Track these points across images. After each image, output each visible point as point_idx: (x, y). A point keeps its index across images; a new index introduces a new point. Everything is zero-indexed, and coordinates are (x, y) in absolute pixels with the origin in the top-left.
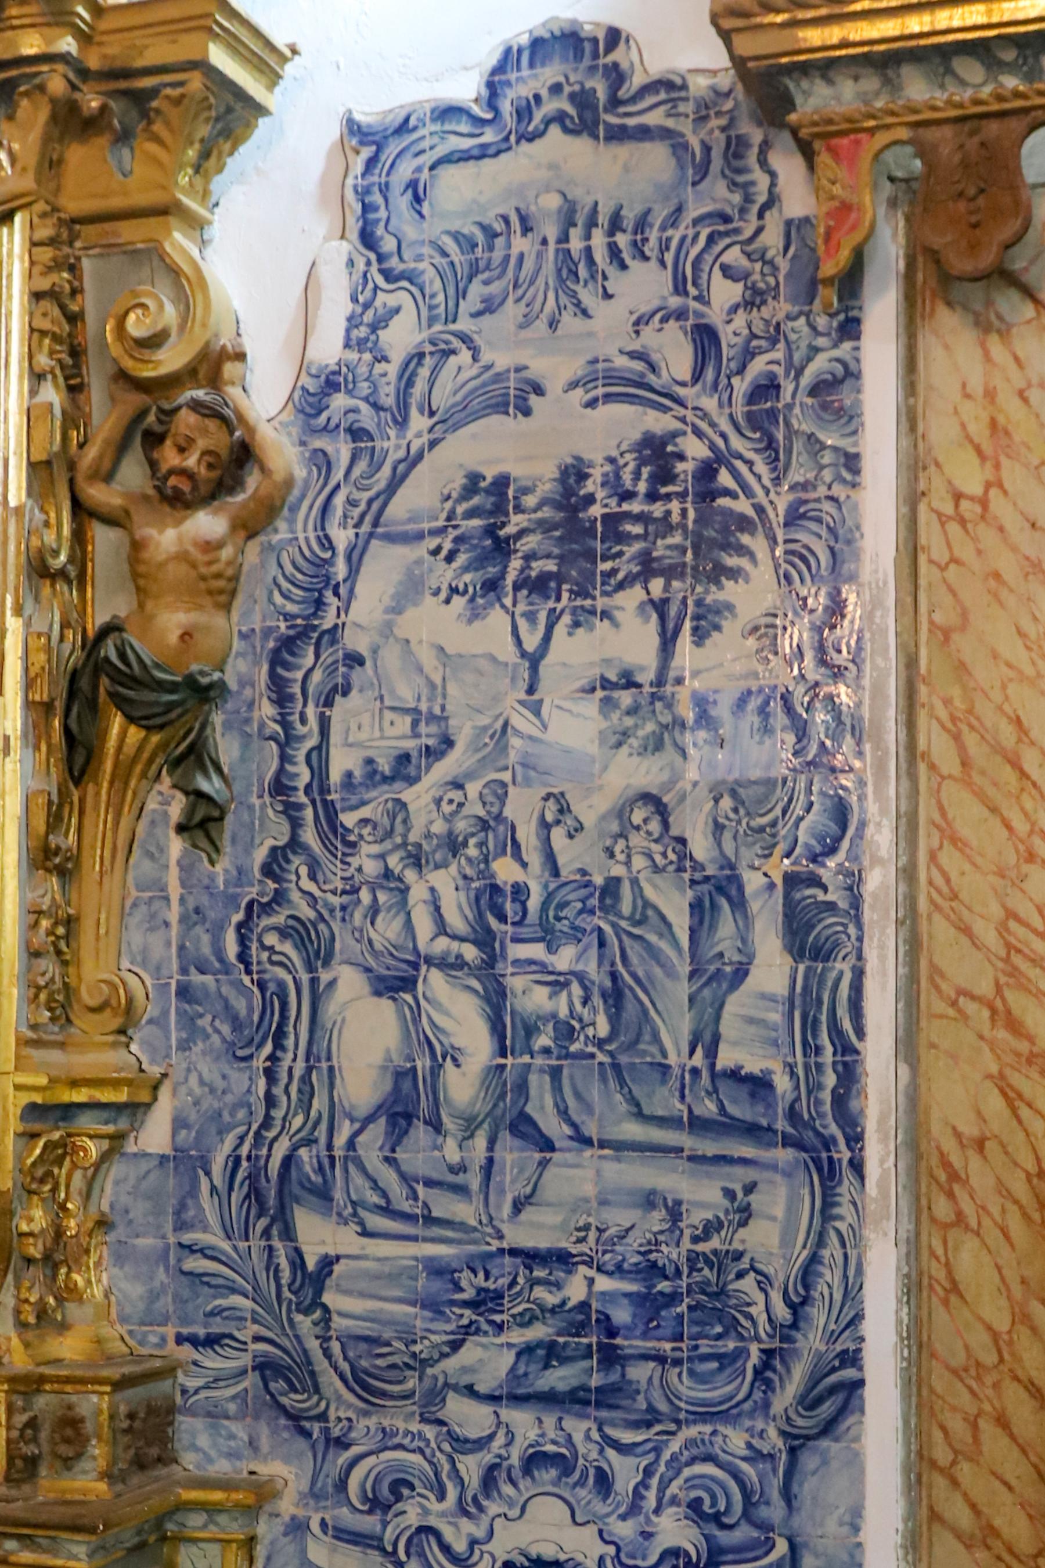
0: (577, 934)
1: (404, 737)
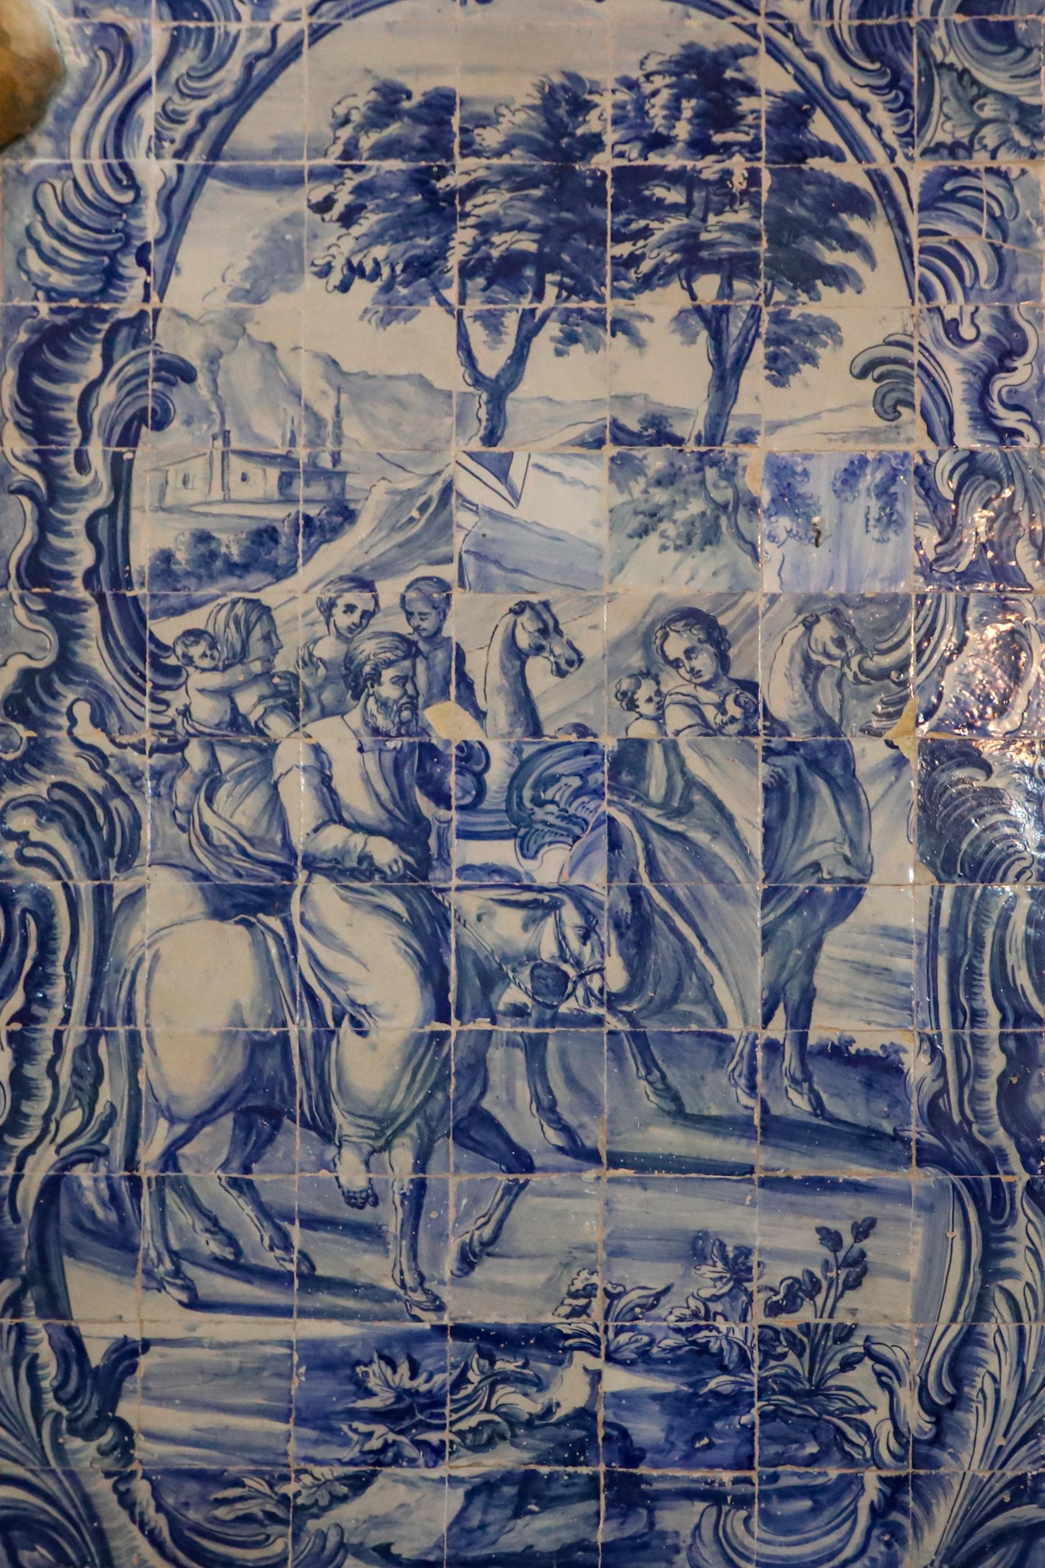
1: (268, 502)
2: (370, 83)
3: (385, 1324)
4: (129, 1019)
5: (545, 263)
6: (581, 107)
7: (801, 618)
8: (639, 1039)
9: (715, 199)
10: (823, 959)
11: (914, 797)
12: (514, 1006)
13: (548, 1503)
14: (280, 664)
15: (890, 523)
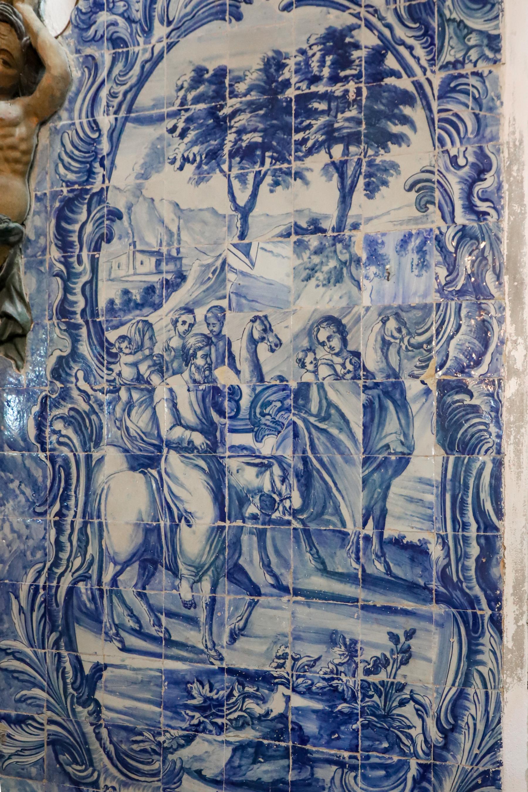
2: (192, 68)
3: (199, 665)
5: (265, 147)
8: (307, 532)
10: (391, 495)
11: (434, 410)
13: (268, 759)
15: (423, 266)
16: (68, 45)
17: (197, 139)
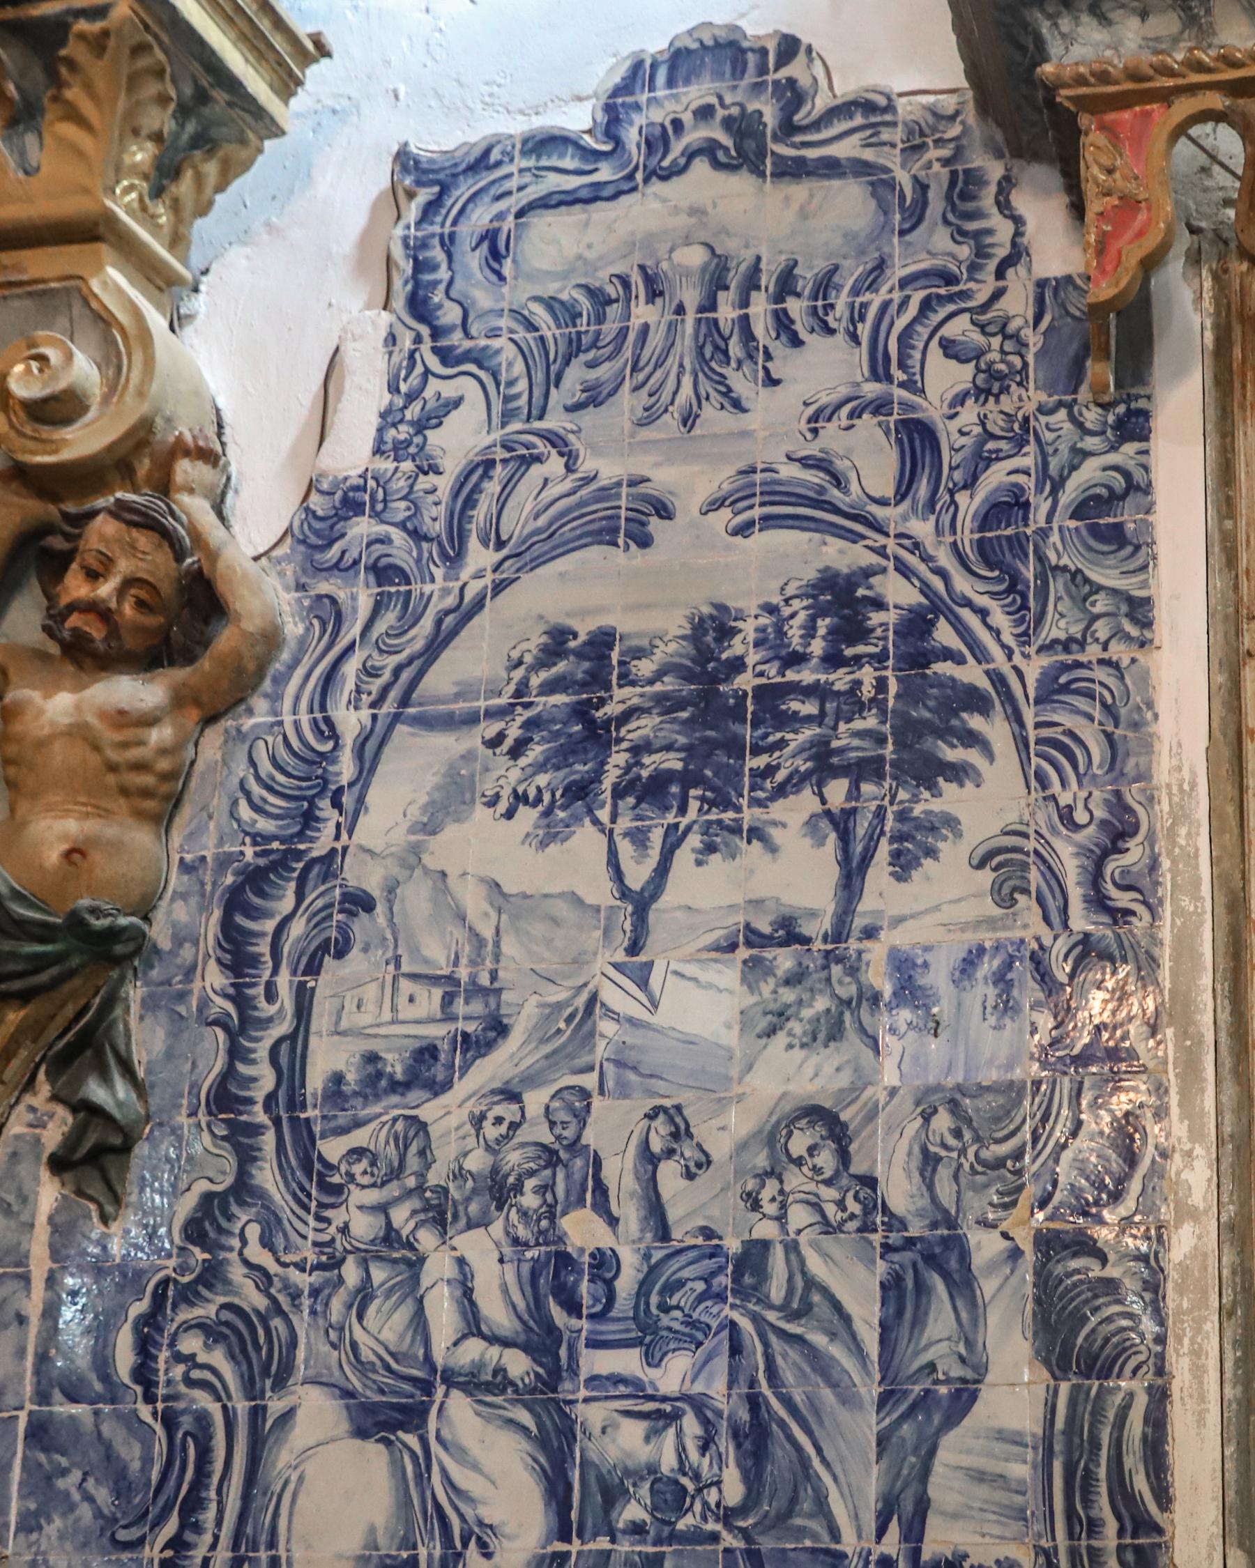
0: (694, 1335)
2: (543, 627)
4: (272, 1544)
5: (688, 779)
6: (726, 633)
7: (919, 1110)
9: (845, 708)
10: (938, 1467)
12: (634, 1523)
14: (433, 1178)
16: (281, 574)
17: (547, 760)
